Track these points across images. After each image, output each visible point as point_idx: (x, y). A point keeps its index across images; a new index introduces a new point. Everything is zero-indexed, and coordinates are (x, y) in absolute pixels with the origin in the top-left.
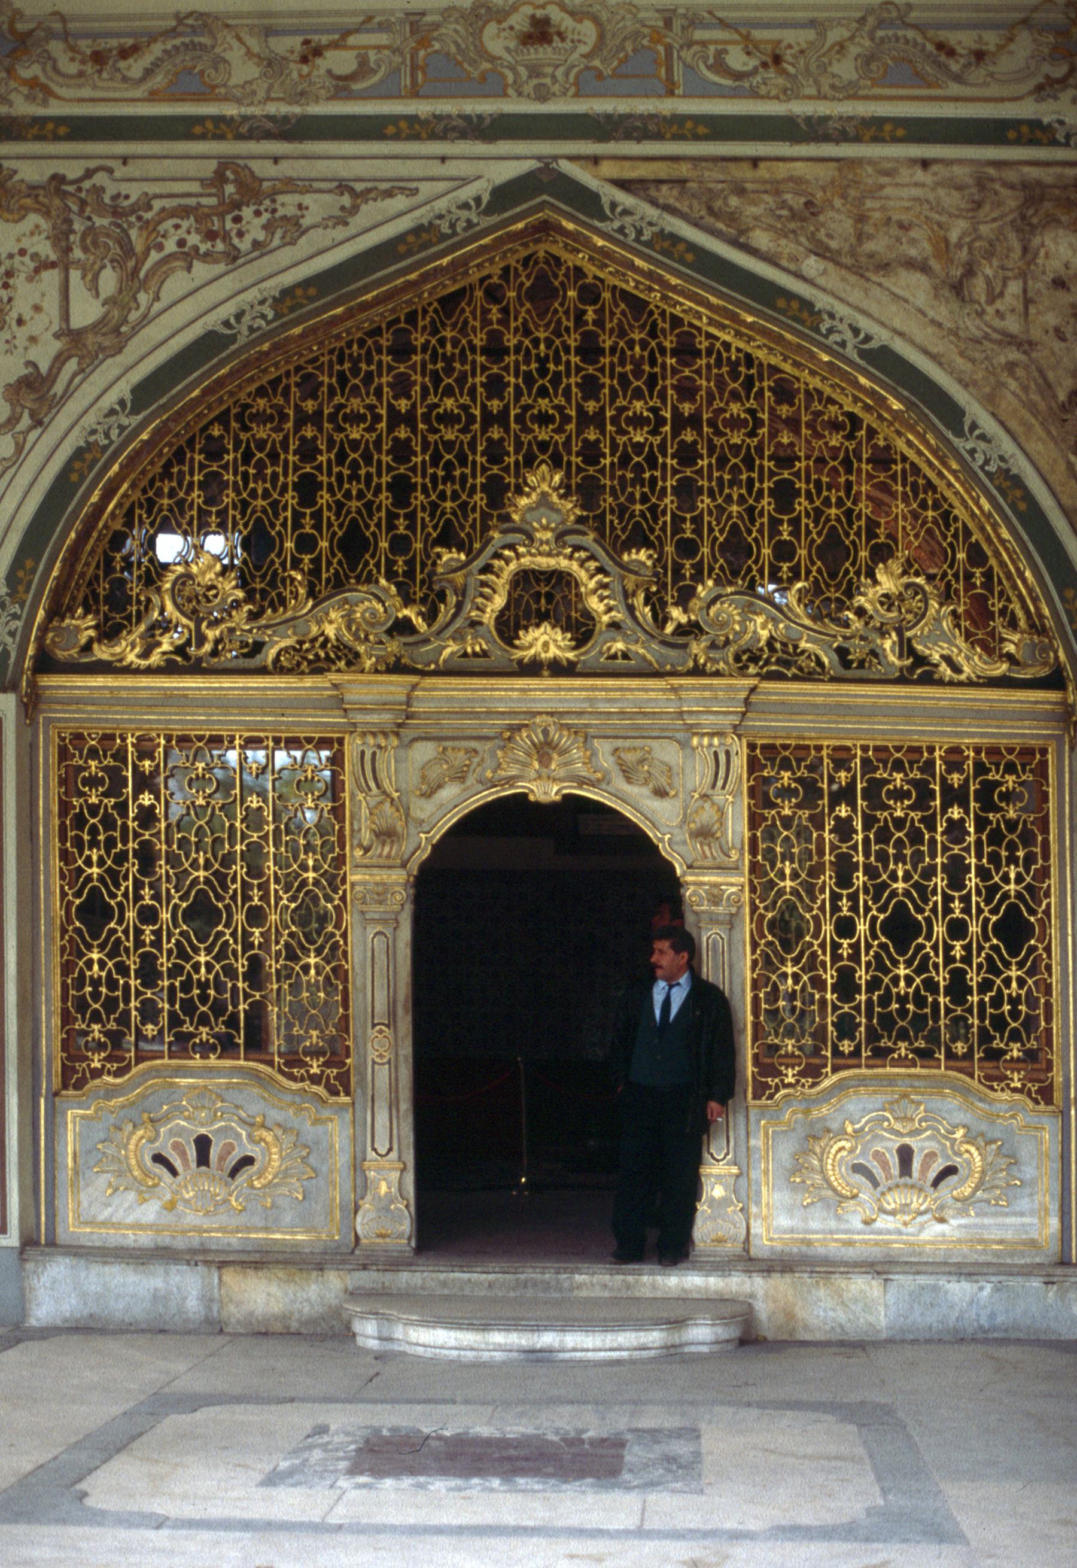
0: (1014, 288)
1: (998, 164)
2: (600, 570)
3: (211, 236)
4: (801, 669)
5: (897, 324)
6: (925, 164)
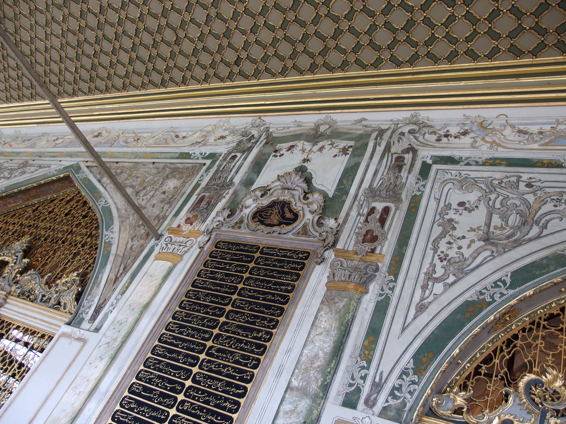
0: (152, 193)
1: (171, 163)
2: (15, 263)
3: (9, 173)
4: (30, 299)
5: (116, 201)
6: (154, 163)
